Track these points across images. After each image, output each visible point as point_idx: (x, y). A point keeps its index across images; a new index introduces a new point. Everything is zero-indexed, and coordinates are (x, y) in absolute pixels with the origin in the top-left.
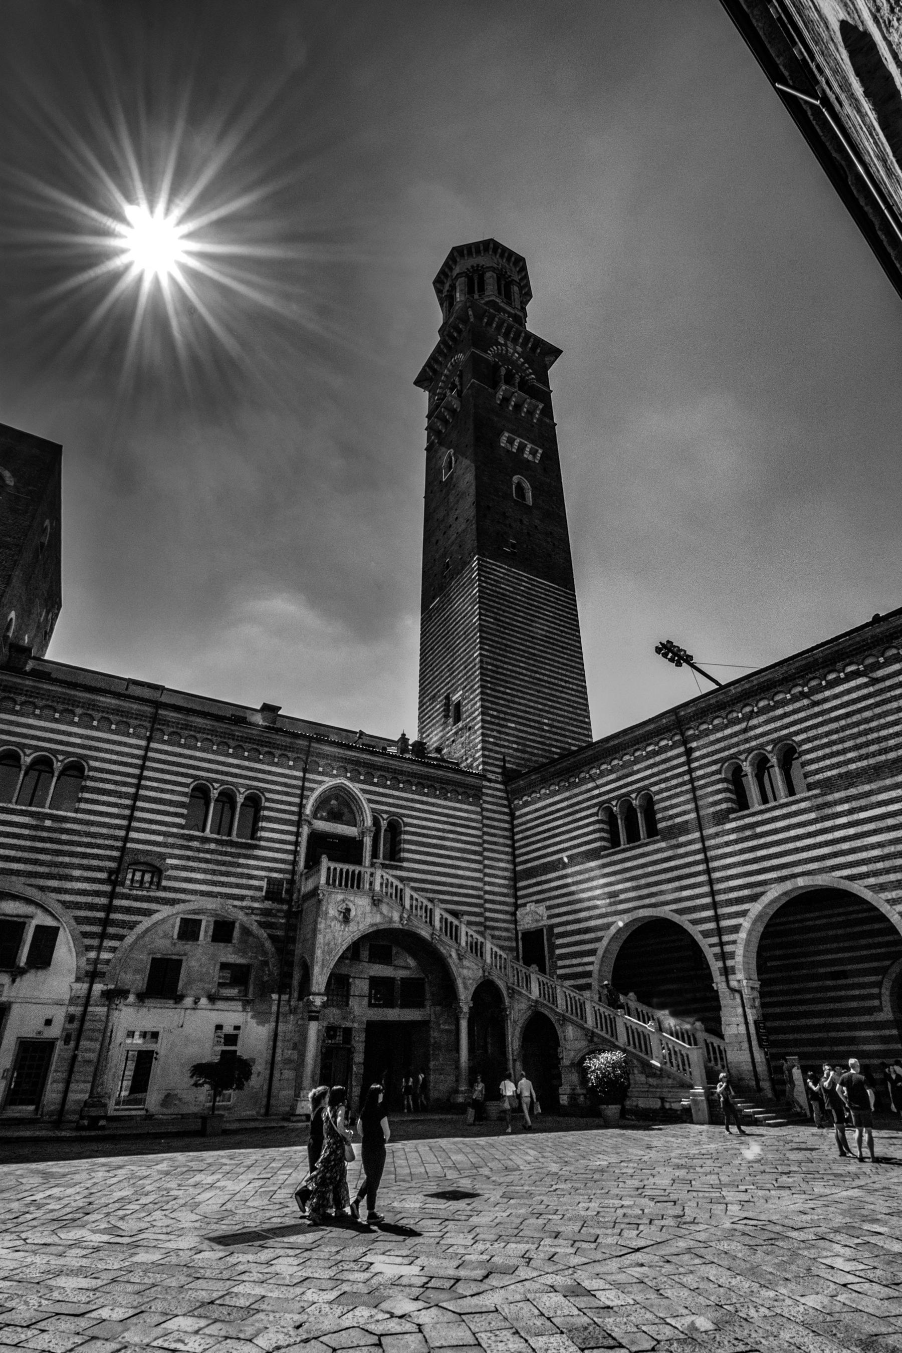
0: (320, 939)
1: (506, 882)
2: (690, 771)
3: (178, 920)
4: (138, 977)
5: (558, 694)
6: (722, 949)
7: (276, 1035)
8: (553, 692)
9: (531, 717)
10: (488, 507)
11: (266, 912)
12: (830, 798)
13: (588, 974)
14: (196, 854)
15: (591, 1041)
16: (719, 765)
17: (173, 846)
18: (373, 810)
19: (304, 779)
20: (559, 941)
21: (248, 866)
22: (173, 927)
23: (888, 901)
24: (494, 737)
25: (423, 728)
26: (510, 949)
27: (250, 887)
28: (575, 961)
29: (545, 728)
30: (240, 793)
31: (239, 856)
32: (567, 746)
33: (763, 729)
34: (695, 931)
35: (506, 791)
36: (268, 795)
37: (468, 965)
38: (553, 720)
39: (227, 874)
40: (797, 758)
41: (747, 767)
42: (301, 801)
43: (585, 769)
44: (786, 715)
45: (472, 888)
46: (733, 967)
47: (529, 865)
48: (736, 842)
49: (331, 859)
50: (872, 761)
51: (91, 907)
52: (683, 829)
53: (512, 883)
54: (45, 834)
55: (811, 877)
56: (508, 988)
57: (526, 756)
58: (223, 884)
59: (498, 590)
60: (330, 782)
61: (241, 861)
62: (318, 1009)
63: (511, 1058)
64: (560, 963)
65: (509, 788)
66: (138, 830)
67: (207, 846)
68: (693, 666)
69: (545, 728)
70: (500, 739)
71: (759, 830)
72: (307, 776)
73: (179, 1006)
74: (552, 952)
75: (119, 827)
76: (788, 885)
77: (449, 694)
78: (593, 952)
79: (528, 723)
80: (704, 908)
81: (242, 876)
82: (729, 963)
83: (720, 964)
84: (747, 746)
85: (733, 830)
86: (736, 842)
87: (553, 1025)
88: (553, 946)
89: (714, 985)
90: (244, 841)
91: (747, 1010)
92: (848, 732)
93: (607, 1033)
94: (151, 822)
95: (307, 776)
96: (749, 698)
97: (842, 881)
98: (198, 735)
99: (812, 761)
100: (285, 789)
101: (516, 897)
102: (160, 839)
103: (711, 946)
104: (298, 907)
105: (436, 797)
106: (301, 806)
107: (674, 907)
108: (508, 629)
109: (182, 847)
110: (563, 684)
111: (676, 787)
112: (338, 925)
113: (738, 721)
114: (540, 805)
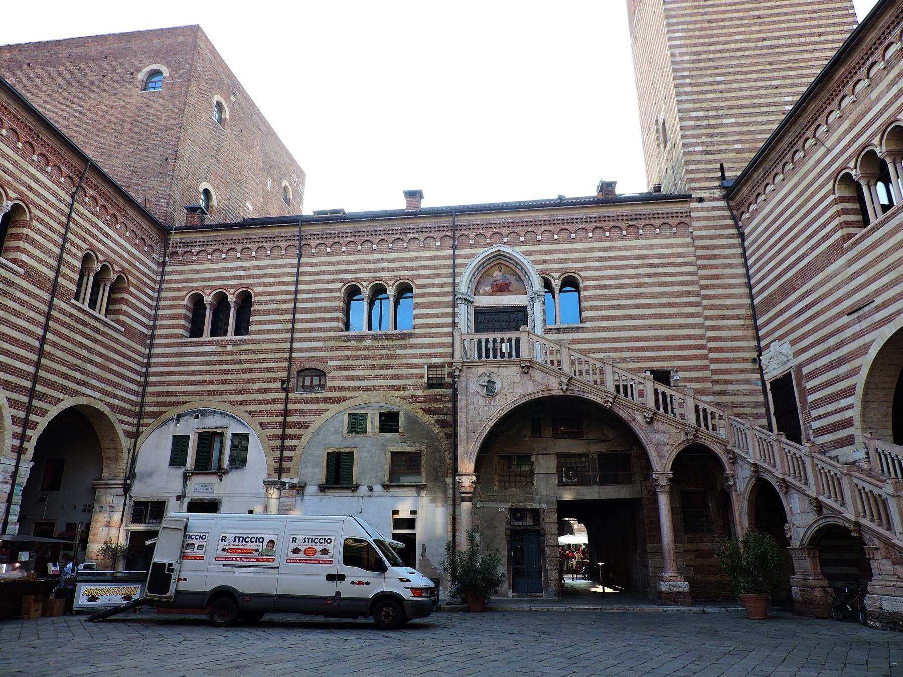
1: (741, 322)
3: (347, 415)
4: (317, 470)
11: (428, 399)
13: (847, 423)
14: (355, 353)
20: (810, 385)
21: (406, 356)
22: (342, 423)
26: (756, 405)
27: (411, 376)
28: (831, 408)
31: (396, 347)
35: (730, 208)
37: (663, 429)
39: (387, 367)
42: (454, 280)
45: (689, 337)
47: (766, 294)
51: (272, 413)
53: (750, 322)
54: (229, 358)
56: (728, 452)
58: (384, 377)
60: (483, 253)
61: (399, 352)
64: (814, 413)
65: (732, 203)
66: (301, 340)
67: (364, 344)
74: (804, 400)
75: (284, 341)
78: (849, 391)
79: (757, 110)
81: (400, 366)
87: (777, 494)
88: (804, 393)
94: (310, 330)
95: (457, 252)
98: (341, 240)
100: (435, 272)
101: (759, 339)
102: (320, 344)
105: (624, 238)
106: (454, 285)
109: (340, 348)
110: (817, 39)
112: (482, 402)
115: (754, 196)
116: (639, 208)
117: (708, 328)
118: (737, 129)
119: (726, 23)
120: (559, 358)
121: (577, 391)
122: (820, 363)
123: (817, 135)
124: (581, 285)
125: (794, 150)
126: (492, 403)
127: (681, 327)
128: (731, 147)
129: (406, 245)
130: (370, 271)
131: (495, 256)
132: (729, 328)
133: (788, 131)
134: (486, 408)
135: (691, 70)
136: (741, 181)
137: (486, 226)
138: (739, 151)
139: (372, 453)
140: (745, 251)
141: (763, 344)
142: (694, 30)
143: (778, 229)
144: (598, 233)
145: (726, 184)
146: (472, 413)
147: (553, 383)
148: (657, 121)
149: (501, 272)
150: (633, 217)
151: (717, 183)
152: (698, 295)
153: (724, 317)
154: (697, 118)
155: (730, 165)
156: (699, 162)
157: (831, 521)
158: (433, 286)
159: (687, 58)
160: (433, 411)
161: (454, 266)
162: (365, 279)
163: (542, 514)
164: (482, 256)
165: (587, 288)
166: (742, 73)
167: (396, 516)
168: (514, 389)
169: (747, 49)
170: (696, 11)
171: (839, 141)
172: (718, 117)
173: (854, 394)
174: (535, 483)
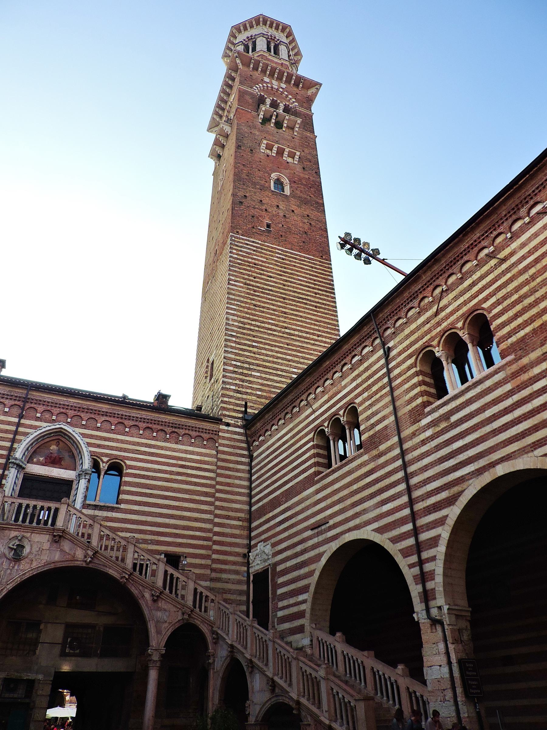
1: (240, 523)
6: (421, 569)
9: (279, 367)
10: (245, 196)
12: (525, 361)
13: (300, 615)
16: (414, 357)
18: (92, 454)
20: (280, 580)
24: (236, 385)
26: (241, 593)
28: (292, 601)
33: (452, 306)
35: (246, 435)
42: (12, 445)
44: (474, 284)
46: (433, 590)
47: (260, 504)
53: (246, 524)
55: (510, 462)
56: (213, 632)
60: (46, 427)
68: (383, 262)
70: (242, 386)
71: (454, 418)
74: (274, 592)
76: (487, 478)
78: (305, 590)
79: (274, 372)
83: (420, 588)
84: (439, 329)
87: (244, 673)
89: (415, 615)
95: (23, 421)
96: (438, 278)
103: (411, 566)
106: (11, 449)
107: (376, 525)
108: (258, 292)
110: (316, 338)
111: (376, 393)
112: (5, 565)
115: (264, 431)
116: (183, 420)
118: (260, 381)
119: (265, 310)
120: (90, 531)
121: (99, 565)
122: (289, 564)
123: (309, 399)
124: (125, 472)
125: (293, 405)
126: (16, 567)
127: (196, 520)
128: (254, 392)
131: (56, 432)
133: (291, 392)
134: (9, 571)
135: (237, 332)
136: (257, 417)
137: (55, 405)
138: (259, 396)
140: (251, 469)
141: (253, 543)
142: (244, 307)
144: (148, 432)
145: (246, 417)
147: (80, 554)
148: (208, 360)
150: (177, 426)
153: (228, 518)
155: (252, 405)
156: (231, 397)
159: (236, 324)
161: (16, 433)
165: (129, 475)
166: (269, 345)
169: (275, 331)
170: (247, 296)
172: (249, 369)
173: (308, 592)
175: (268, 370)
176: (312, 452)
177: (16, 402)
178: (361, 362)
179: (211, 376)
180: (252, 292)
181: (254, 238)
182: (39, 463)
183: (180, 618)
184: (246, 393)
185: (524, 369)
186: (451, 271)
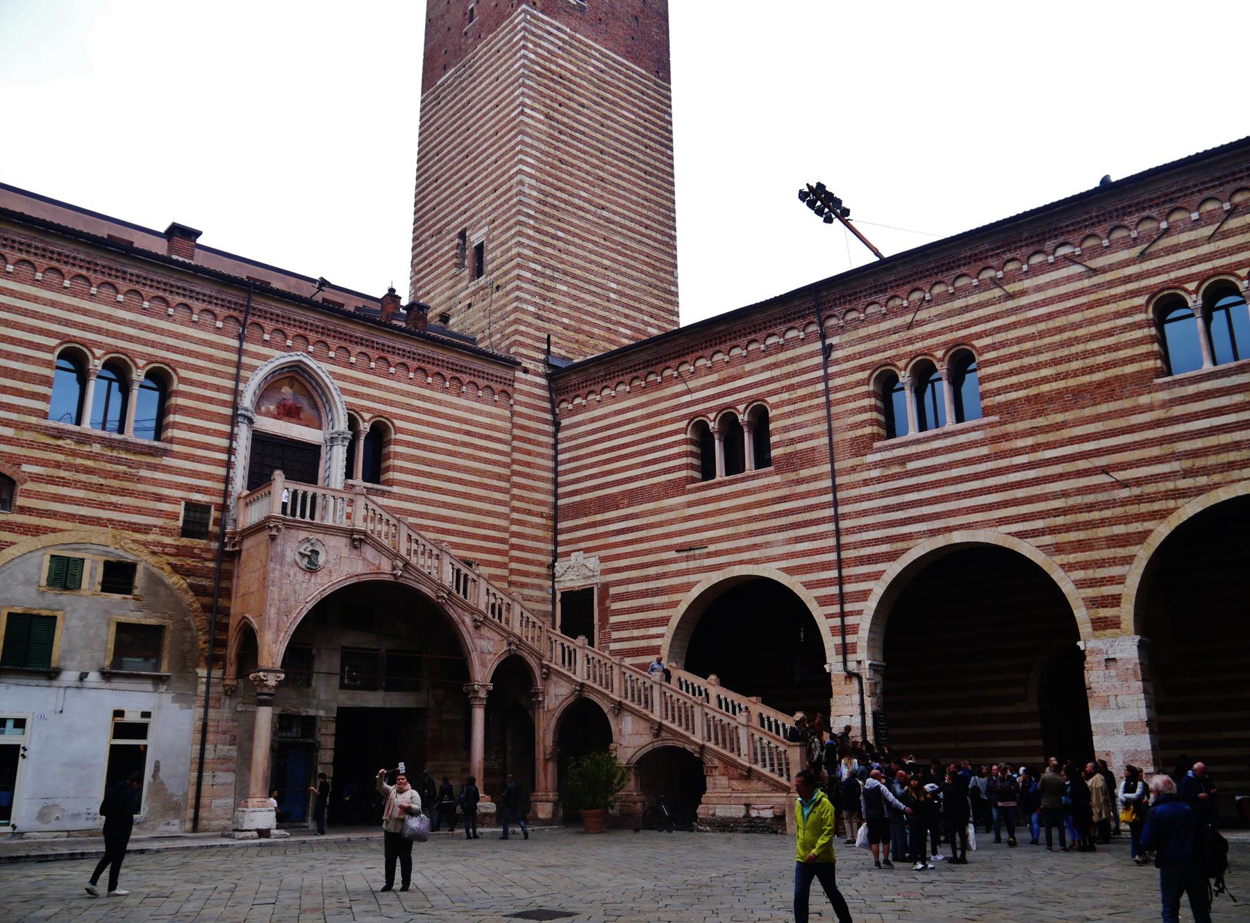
0: (274, 592)
1: (543, 521)
2: (826, 378)
3: (47, 558)
5: (634, 245)
6: (843, 621)
7: (205, 725)
8: (628, 243)
9: (592, 277)
11: (181, 551)
12: (1010, 428)
13: (655, 650)
14: (70, 459)
15: (657, 735)
16: (868, 372)
17: (31, 445)
19: (240, 351)
20: (616, 606)
21: (155, 482)
22: (40, 568)
23: (1062, 566)
25: (418, 280)
26: (545, 614)
28: (636, 633)
29: (612, 296)
30: (138, 368)
31: (140, 465)
32: (642, 326)
33: (933, 324)
34: (808, 597)
35: (549, 389)
36: (183, 373)
38: (625, 285)
39: (123, 492)
40: (975, 370)
41: (904, 377)
42: (237, 385)
43: (672, 363)
44: (967, 309)
45: (494, 527)
46: (854, 645)
47: (577, 498)
48: (878, 480)
49: (289, 477)
50: (1071, 382)
52: (807, 458)
53: (550, 523)
55: (971, 532)
57: (581, 337)
59: (553, 67)
60: (280, 358)
61: (143, 473)
62: (272, 691)
63: (542, 756)
64: (615, 635)
67: (87, 448)
68: (847, 224)
69: (612, 296)
70: (544, 308)
71: (911, 466)
72: (246, 346)
73: (55, 683)
77: (465, 230)
78: (664, 621)
79: (586, 286)
80: (824, 566)
81: (145, 495)
82: (850, 639)
84: (909, 348)
85: (876, 465)
86: (878, 480)
87: (605, 715)
90: (146, 442)
91: (865, 697)
92: (1047, 340)
93: (680, 725)
95: (246, 346)
96: (920, 279)
97: (1010, 538)
98: (65, 269)
99: (993, 377)
103: (828, 616)
104: (234, 546)
105: (445, 390)
106: (236, 393)
107: (784, 564)
109: (46, 447)
110: (643, 230)
112: (300, 575)
113: (903, 311)
114: (609, 410)
115: (586, 391)
117: (513, 522)
118: (568, 300)
119: (575, 171)
122: (633, 588)
124: (393, 437)
126: (313, 580)
129: (171, 311)
130: (107, 333)
132: (533, 526)
133: (649, 348)
138: (566, 327)
139: (86, 622)
141: (560, 549)
142: (546, 163)
143: (610, 438)
144: (420, 375)
146: (287, 588)
147: (386, 565)
149: (297, 390)
151: (542, 357)
152: (508, 480)
153: (529, 512)
154: (534, 272)
157: (670, 743)
158: (205, 385)
159: (534, 193)
160: (188, 570)
162: (100, 345)
163: (319, 723)
164: (277, 363)
166: (581, 237)
167: (118, 719)
168: (342, 567)
169: (588, 212)
171: (703, 388)
172: (552, 279)
174: (313, 683)
175: (577, 282)
176: (684, 448)
177: (231, 312)
178: (782, 348)
179: (478, 271)
180: (556, 134)
181: (560, 21)
182: (268, 414)
183: (506, 648)
184: (549, 320)
185: (1006, 437)
186: (940, 277)
